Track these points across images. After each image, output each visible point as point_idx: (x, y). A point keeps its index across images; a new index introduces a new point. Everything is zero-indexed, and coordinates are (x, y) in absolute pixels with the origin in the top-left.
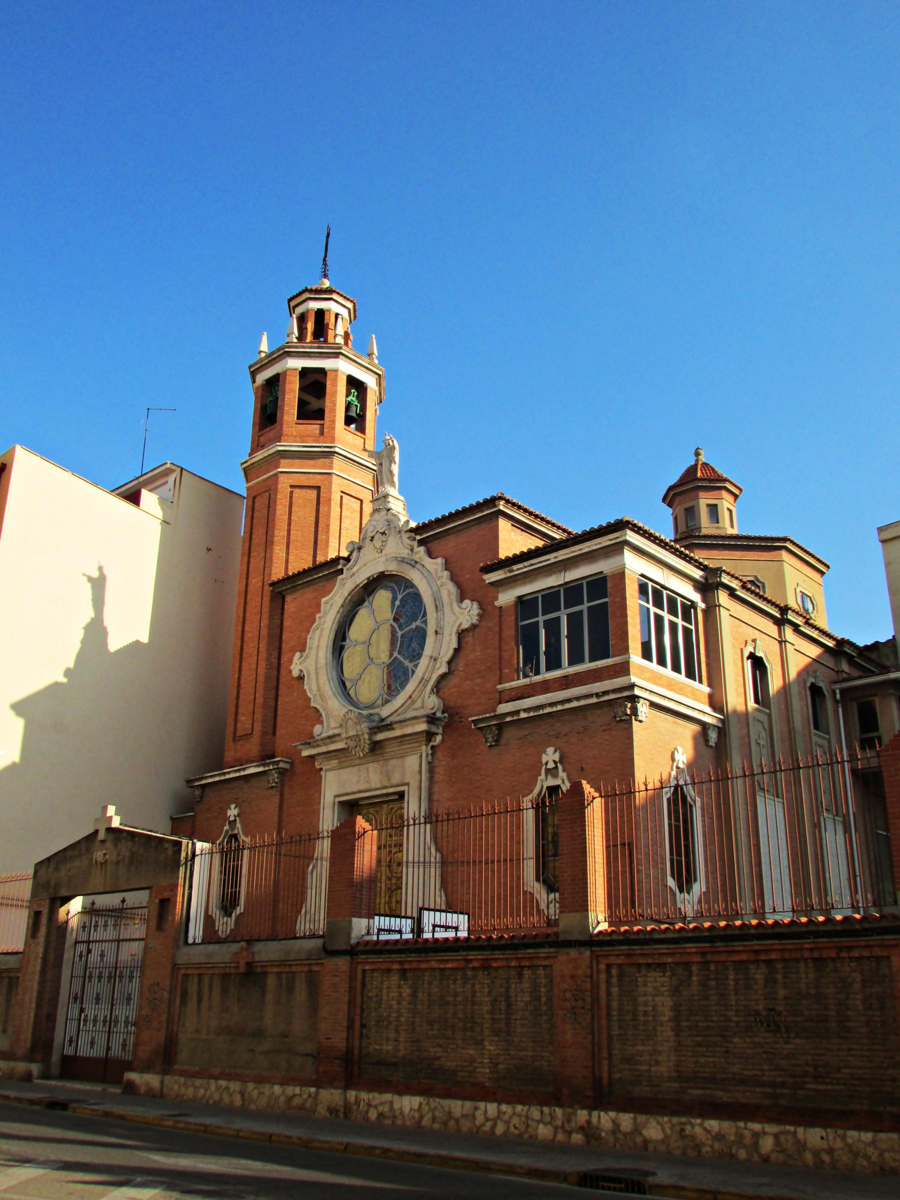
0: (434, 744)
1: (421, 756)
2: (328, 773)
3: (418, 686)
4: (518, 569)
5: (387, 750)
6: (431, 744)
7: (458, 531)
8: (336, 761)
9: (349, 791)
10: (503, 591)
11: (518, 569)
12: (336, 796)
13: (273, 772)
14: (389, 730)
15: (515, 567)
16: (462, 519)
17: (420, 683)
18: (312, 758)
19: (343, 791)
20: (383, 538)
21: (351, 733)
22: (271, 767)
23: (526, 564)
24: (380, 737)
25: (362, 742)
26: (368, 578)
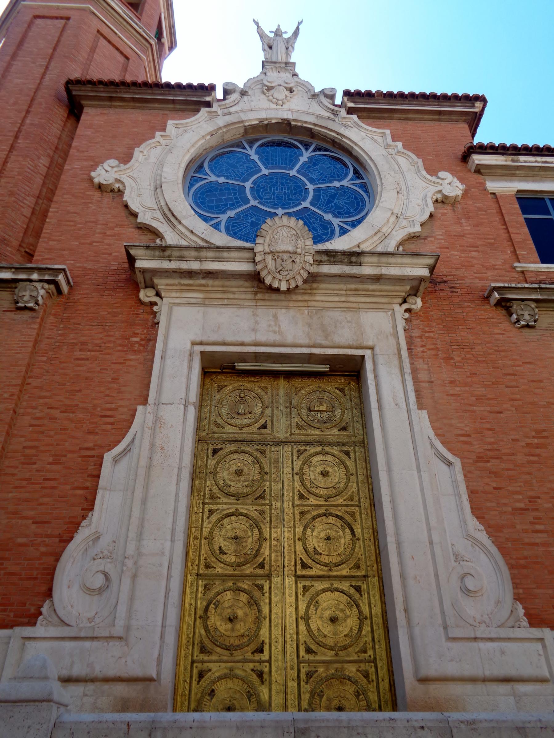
0: (413, 307)
1: (394, 316)
2: (176, 309)
3: (372, 237)
4: (525, 162)
5: (318, 298)
6: (405, 306)
7: (407, 119)
8: (201, 295)
9: (230, 338)
10: (493, 181)
11: (525, 162)
12: (194, 344)
13: (39, 285)
14: (351, 263)
15: (522, 158)
16: (423, 105)
17: (376, 234)
18: (155, 272)
19: (214, 338)
20: (287, 93)
21: (283, 247)
22: (35, 276)
23: (539, 159)
24: (326, 269)
25: (297, 267)
26: (261, 121)
